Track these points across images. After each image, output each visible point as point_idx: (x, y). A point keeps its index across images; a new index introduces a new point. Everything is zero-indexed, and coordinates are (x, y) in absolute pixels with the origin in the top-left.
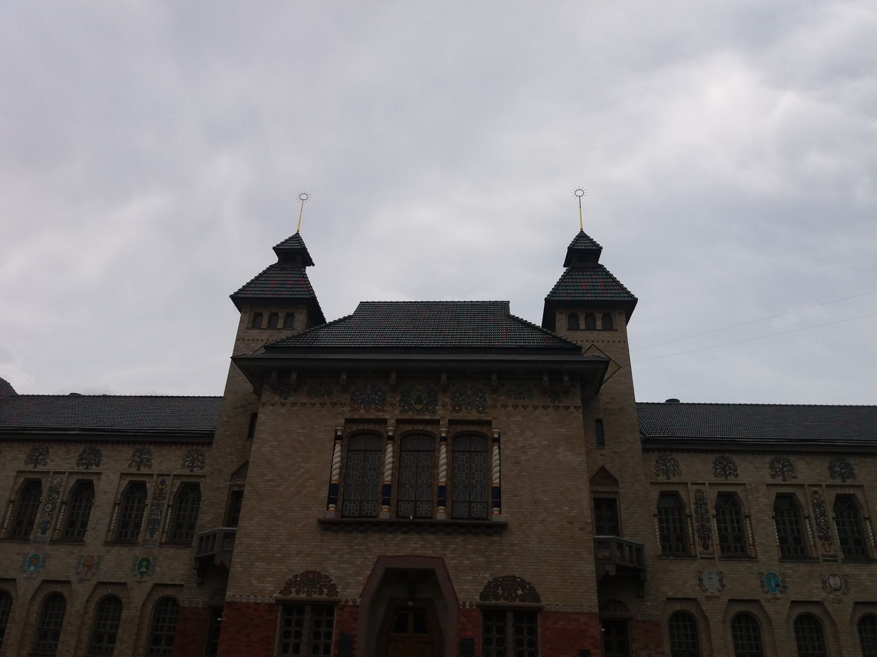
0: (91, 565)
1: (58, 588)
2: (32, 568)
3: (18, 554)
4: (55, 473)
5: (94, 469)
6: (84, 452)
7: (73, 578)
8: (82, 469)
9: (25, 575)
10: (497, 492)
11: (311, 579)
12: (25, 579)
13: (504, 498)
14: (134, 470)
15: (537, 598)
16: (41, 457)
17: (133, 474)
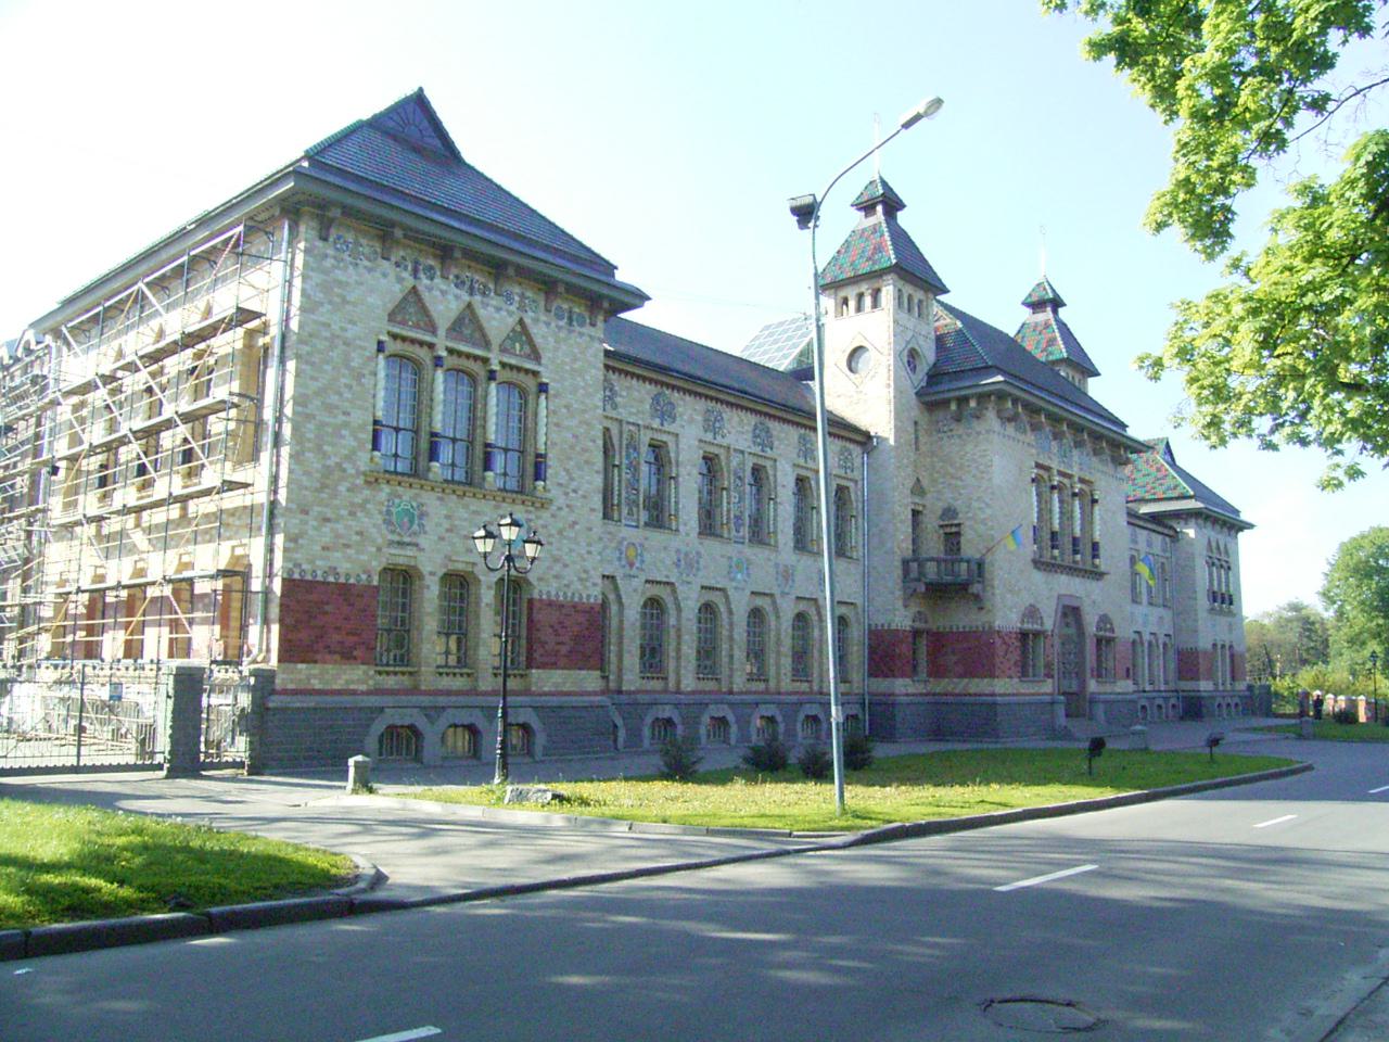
0: (787, 575)
1: (759, 602)
2: (739, 576)
3: (722, 556)
4: (735, 450)
5: (769, 453)
6: (756, 427)
7: (776, 591)
8: (757, 450)
9: (734, 584)
10: (1095, 546)
11: (1032, 613)
12: (736, 588)
13: (1102, 552)
14: (801, 461)
15: (1112, 630)
16: (717, 425)
17: (802, 467)
